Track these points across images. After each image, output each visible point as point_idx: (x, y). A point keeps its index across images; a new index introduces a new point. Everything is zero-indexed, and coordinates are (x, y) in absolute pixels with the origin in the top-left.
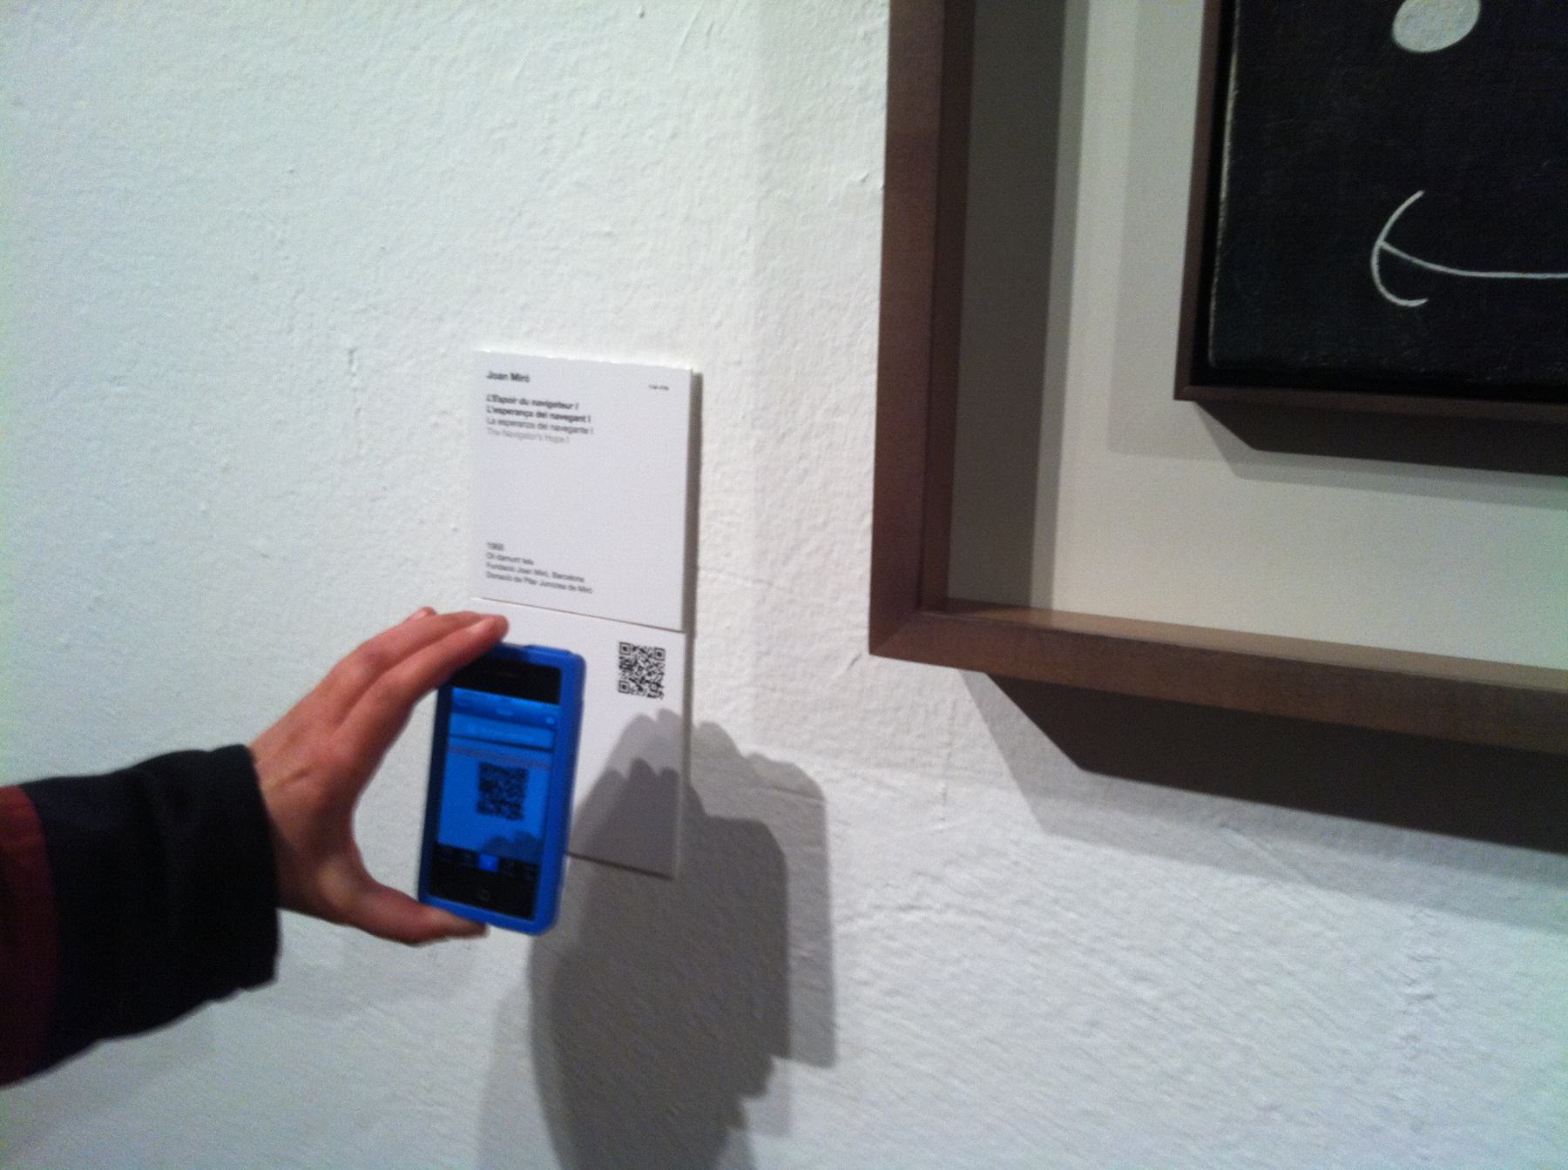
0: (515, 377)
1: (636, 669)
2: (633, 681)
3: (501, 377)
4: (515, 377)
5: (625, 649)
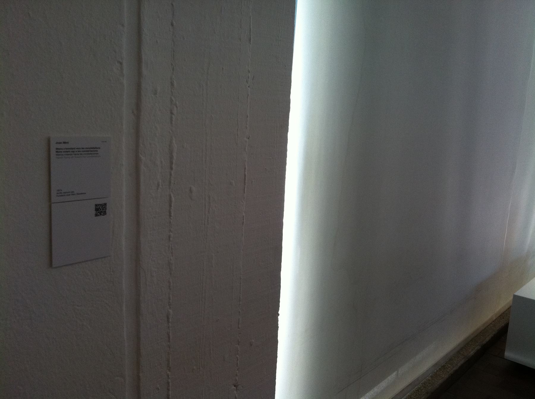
0: (65, 143)
1: (99, 210)
2: (99, 213)
3: (60, 143)
4: (65, 143)
5: (96, 206)
